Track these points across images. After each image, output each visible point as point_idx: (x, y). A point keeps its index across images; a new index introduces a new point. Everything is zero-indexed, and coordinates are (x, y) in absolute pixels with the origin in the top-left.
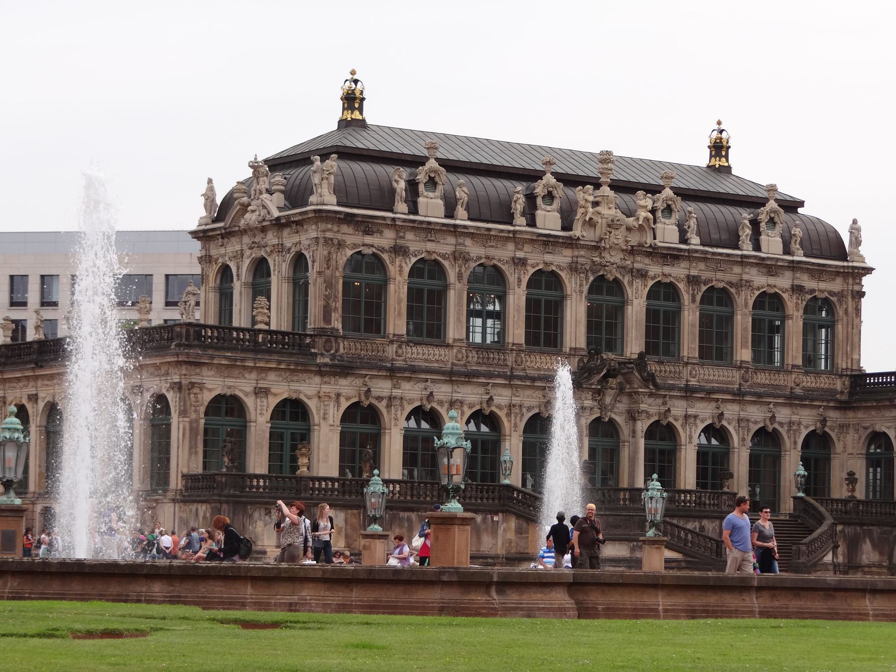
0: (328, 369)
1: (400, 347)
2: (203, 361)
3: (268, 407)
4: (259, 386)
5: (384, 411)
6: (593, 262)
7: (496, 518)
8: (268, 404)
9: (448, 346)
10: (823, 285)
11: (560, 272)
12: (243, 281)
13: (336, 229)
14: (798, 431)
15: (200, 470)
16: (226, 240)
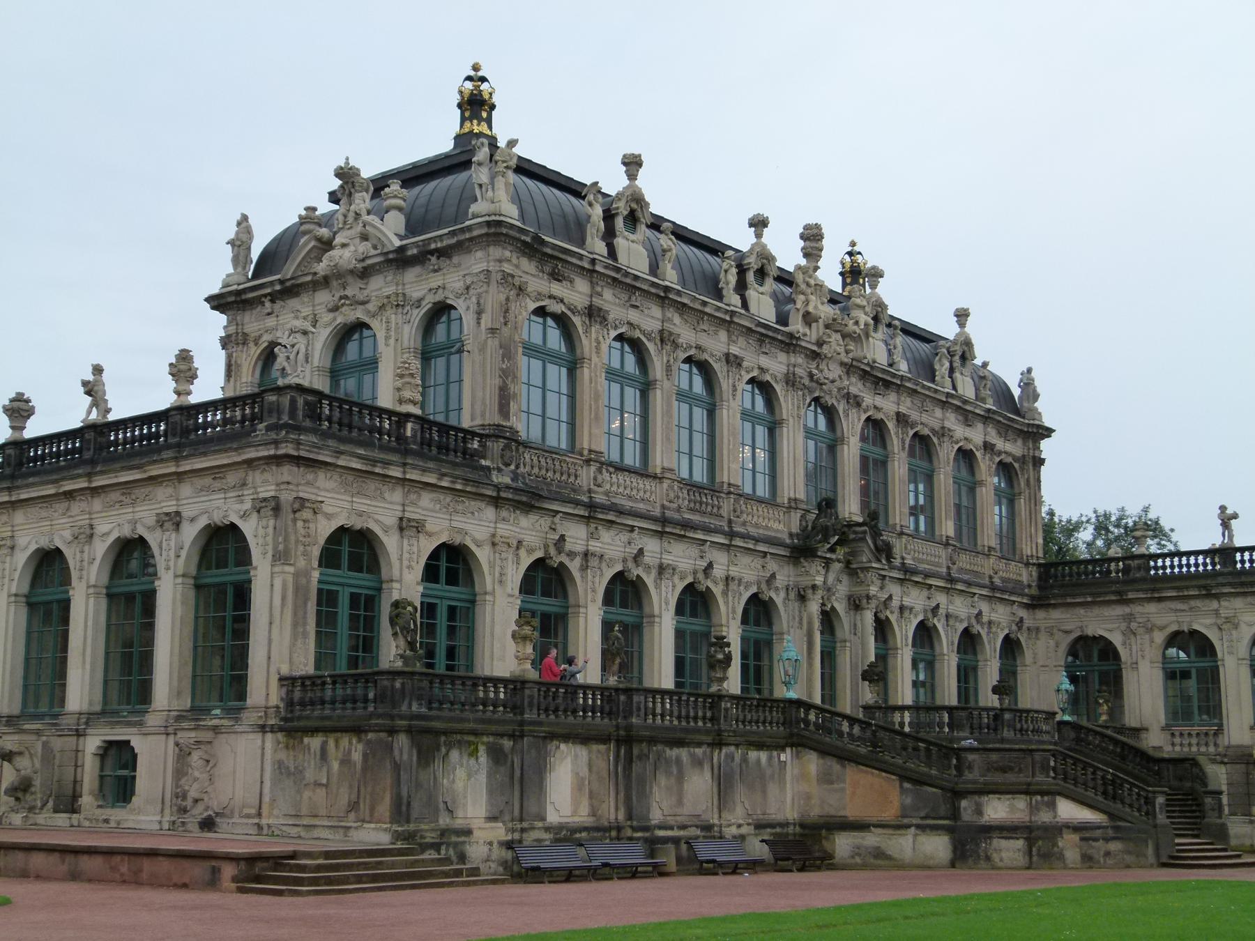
0: (510, 496)
1: (600, 470)
2: (321, 458)
3: (419, 556)
4: (407, 515)
5: (576, 574)
6: (811, 376)
7: (783, 757)
8: (419, 551)
9: (655, 477)
10: (1009, 447)
11: (774, 385)
12: (316, 364)
13: (515, 261)
14: (996, 634)
15: (310, 669)
16: (279, 304)
